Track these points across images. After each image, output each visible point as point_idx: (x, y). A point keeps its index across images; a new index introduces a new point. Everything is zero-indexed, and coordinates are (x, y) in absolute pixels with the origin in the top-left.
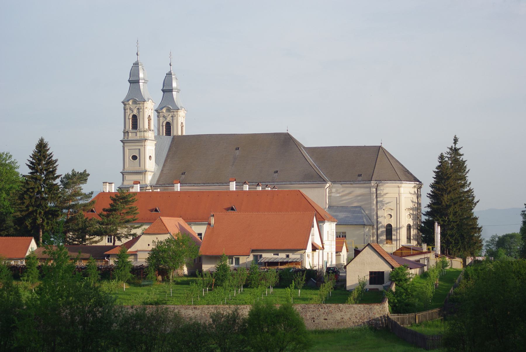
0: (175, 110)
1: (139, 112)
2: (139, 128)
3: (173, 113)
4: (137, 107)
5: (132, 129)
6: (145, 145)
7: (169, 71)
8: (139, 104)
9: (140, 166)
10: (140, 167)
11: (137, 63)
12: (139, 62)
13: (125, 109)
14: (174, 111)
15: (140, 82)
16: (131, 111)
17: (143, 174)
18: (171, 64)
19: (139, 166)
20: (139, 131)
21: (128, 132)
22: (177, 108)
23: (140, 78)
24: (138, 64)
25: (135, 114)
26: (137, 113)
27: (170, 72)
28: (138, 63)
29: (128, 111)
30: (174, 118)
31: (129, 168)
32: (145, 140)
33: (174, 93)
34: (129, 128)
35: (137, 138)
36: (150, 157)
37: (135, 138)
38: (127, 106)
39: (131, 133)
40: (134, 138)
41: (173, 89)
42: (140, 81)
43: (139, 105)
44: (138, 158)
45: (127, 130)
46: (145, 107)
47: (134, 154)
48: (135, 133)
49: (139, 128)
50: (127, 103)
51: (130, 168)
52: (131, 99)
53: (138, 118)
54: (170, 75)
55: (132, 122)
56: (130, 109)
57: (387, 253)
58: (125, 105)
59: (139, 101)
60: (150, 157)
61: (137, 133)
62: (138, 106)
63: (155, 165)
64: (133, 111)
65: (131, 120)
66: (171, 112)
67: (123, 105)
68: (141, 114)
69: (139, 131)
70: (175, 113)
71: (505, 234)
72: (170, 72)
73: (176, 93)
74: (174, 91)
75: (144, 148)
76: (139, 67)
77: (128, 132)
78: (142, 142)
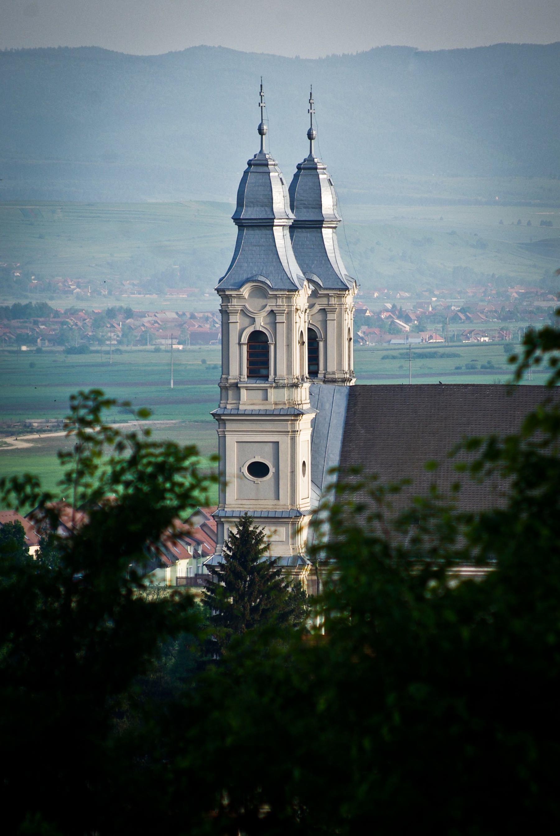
0: (333, 289)
1: (274, 324)
2: (275, 374)
3: (324, 301)
4: (268, 309)
5: (248, 377)
6: (294, 431)
7: (306, 157)
8: (276, 297)
9: (278, 498)
10: (276, 502)
11: (264, 162)
12: (267, 156)
13: (225, 313)
14: (331, 293)
15: (275, 224)
16: (247, 321)
17: (287, 523)
18: (314, 132)
19: (272, 494)
20: (274, 385)
21: (236, 387)
22: (340, 284)
23: (274, 210)
24: (267, 165)
25: (261, 329)
26: (268, 327)
27: (310, 159)
28: (267, 160)
29: (236, 319)
30: (330, 316)
31: (240, 502)
32: (298, 415)
33: (327, 233)
34: (241, 374)
35: (268, 407)
36: (304, 463)
37: (262, 407)
38: (235, 302)
39: (247, 389)
40: (256, 407)
41: (323, 221)
42: (276, 222)
43: (274, 300)
44: (272, 470)
45: (236, 381)
46: (294, 308)
47: (258, 459)
48: (260, 393)
49: (275, 374)
50: (233, 293)
51: (244, 502)
52: (247, 281)
53: (270, 342)
54: (313, 172)
55: (250, 354)
56: (244, 312)
57: (308, 413)
58: (226, 298)
59: (277, 290)
60: (304, 463)
61: (269, 390)
62: (271, 305)
63: (311, 486)
64: (253, 320)
65: (245, 348)
66: (320, 297)
67: (219, 300)
68: (281, 329)
69: (274, 385)
70: (333, 301)
71: (43, 48)
72: (310, 159)
73: (330, 230)
74: (325, 227)
75: (293, 439)
76: (271, 174)
77: (236, 387)
78: (287, 420)
